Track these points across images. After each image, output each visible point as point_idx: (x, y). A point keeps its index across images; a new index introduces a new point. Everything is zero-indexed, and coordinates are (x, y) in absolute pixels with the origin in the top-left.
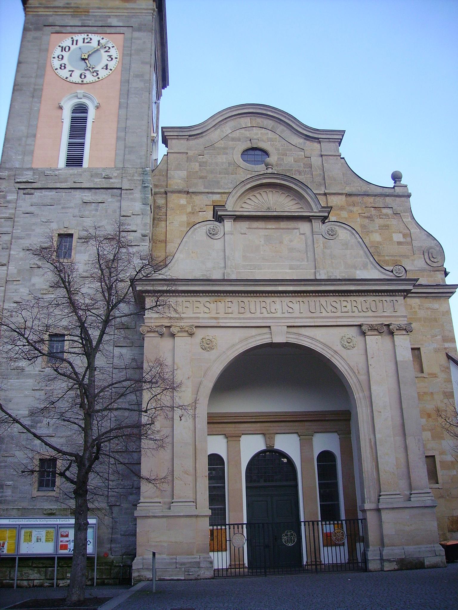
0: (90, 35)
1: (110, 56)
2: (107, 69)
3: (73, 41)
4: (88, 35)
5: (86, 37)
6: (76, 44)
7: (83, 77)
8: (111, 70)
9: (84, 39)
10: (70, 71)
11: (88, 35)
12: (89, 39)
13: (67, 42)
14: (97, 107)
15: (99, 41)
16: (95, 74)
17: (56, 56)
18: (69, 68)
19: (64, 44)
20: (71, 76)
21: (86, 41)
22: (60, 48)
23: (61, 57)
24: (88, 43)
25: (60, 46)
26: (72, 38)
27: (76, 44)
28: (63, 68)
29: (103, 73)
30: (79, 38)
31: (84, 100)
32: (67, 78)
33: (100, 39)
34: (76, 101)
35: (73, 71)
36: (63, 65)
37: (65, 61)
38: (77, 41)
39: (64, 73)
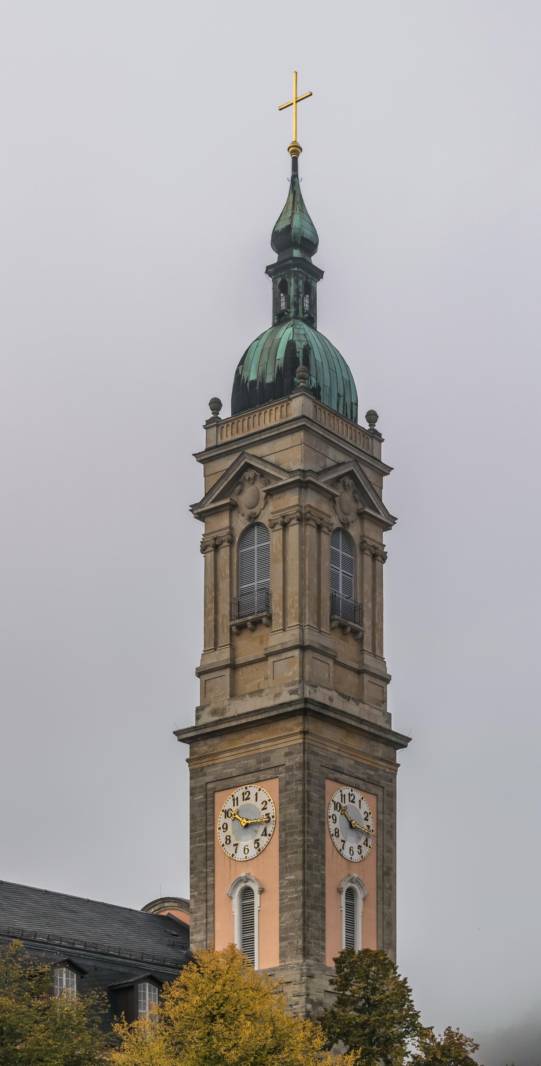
0: (248, 786)
1: (267, 814)
2: (266, 835)
3: (234, 800)
4: (246, 788)
5: (244, 790)
6: (237, 805)
7: (246, 851)
8: (270, 835)
9: (243, 794)
10: (234, 845)
11: (246, 788)
12: (248, 793)
13: (229, 805)
14: (262, 891)
15: (256, 794)
16: (256, 845)
17: (221, 826)
18: (234, 841)
19: (226, 808)
20: (236, 852)
21: (246, 796)
22: (223, 814)
23: (225, 826)
24: (248, 799)
25: (223, 811)
26: (233, 796)
27: (237, 805)
28: (228, 842)
29: (264, 841)
30: (238, 793)
31: (249, 884)
32: (233, 855)
33: (257, 790)
34: (242, 885)
35: (237, 845)
36: (228, 838)
37: (230, 832)
38: (237, 799)
39: (230, 849)
